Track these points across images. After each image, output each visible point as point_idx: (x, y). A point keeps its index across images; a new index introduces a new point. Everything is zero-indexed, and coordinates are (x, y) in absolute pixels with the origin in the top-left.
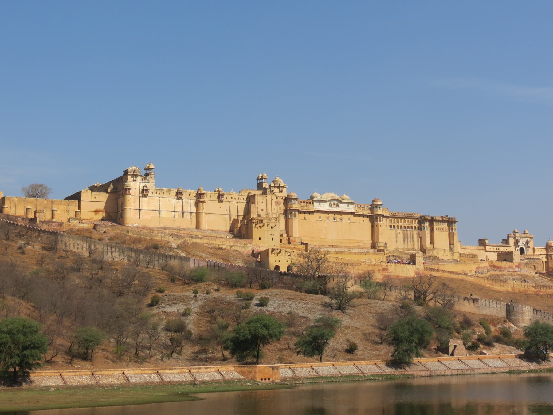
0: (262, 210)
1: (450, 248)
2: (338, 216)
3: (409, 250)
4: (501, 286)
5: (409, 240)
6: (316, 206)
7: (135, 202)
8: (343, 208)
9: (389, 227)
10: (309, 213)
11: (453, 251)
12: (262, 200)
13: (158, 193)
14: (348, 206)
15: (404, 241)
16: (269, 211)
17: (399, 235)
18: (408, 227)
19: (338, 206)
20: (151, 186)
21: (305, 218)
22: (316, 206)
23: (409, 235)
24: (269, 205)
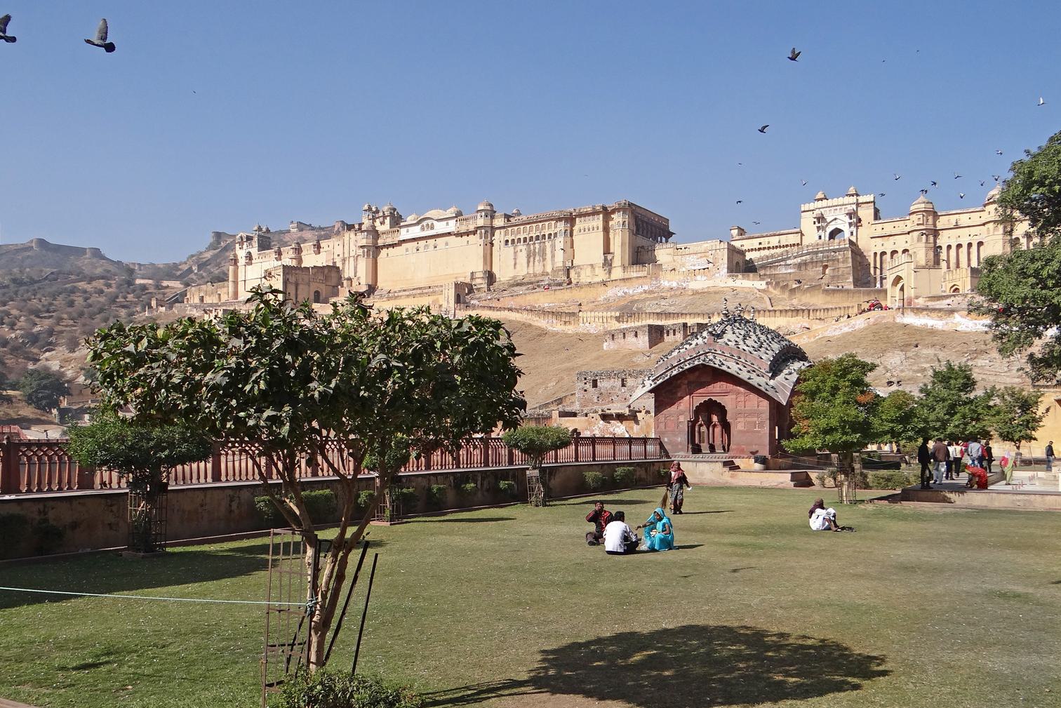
0: (338, 255)
1: (606, 259)
2: (431, 242)
3: (535, 276)
4: (565, 322)
5: (537, 258)
6: (404, 234)
8: (440, 228)
9: (503, 243)
11: (611, 265)
15: (528, 262)
16: (346, 255)
17: (519, 253)
18: (537, 238)
19: (432, 228)
23: (537, 251)
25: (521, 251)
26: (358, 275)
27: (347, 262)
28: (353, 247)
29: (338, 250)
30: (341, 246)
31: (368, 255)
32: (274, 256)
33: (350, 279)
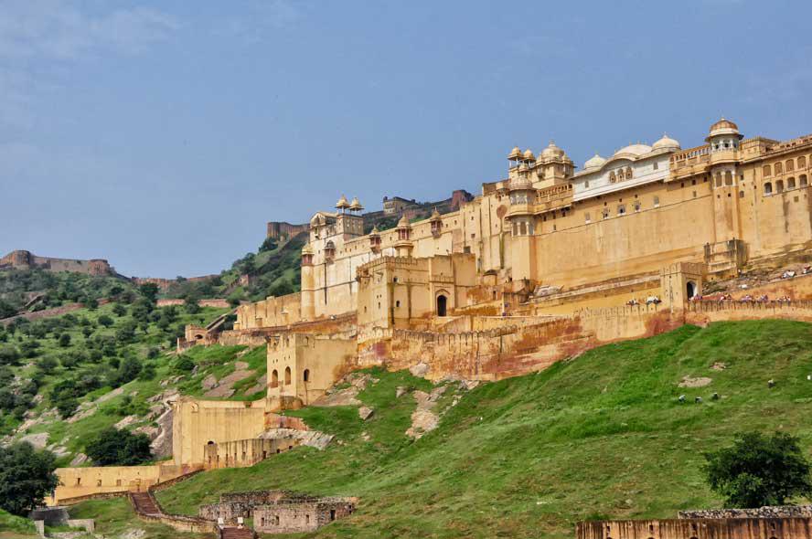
0: (473, 235)
2: (629, 202)
6: (580, 192)
7: (320, 275)
8: (643, 175)
9: (761, 188)
10: (565, 211)
12: (472, 214)
13: (348, 250)
14: (656, 167)
16: (486, 234)
17: (794, 206)
19: (629, 176)
20: (338, 240)
21: (555, 227)
22: (580, 192)
24: (485, 221)
25: (796, 199)
26: (507, 264)
27: (487, 246)
28: (496, 220)
29: (473, 227)
30: (477, 219)
31: (523, 231)
32: (368, 244)
33: (492, 272)
